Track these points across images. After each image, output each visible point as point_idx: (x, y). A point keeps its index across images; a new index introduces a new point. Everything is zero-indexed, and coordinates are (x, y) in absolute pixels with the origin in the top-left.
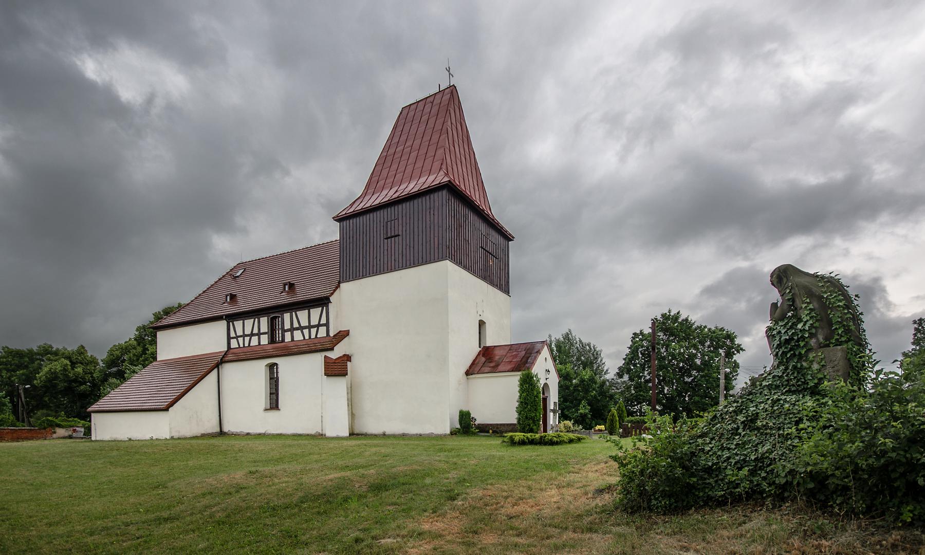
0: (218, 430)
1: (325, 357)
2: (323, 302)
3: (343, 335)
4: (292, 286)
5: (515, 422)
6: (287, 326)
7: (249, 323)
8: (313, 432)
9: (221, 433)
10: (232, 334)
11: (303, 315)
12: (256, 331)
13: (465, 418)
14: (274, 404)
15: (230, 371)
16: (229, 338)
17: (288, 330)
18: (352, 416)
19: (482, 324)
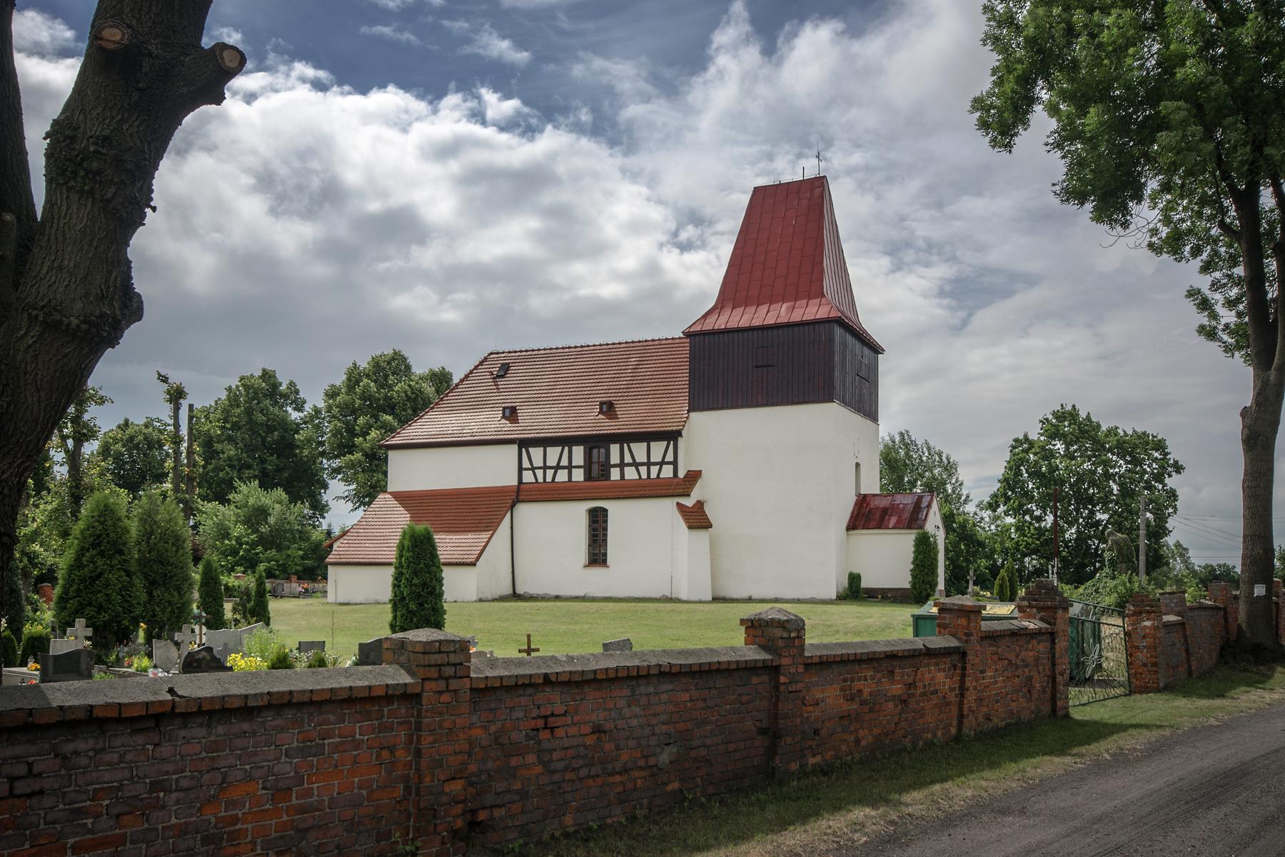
0: (510, 591)
1: (678, 504)
2: (672, 436)
3: (693, 477)
4: (610, 405)
5: (908, 586)
6: (615, 459)
7: (553, 453)
8: (658, 595)
9: (515, 596)
10: (526, 464)
11: (639, 450)
12: (564, 462)
13: (854, 579)
14: (597, 557)
15: (526, 512)
16: (521, 469)
17: (615, 466)
18: (714, 577)
19: (858, 465)
